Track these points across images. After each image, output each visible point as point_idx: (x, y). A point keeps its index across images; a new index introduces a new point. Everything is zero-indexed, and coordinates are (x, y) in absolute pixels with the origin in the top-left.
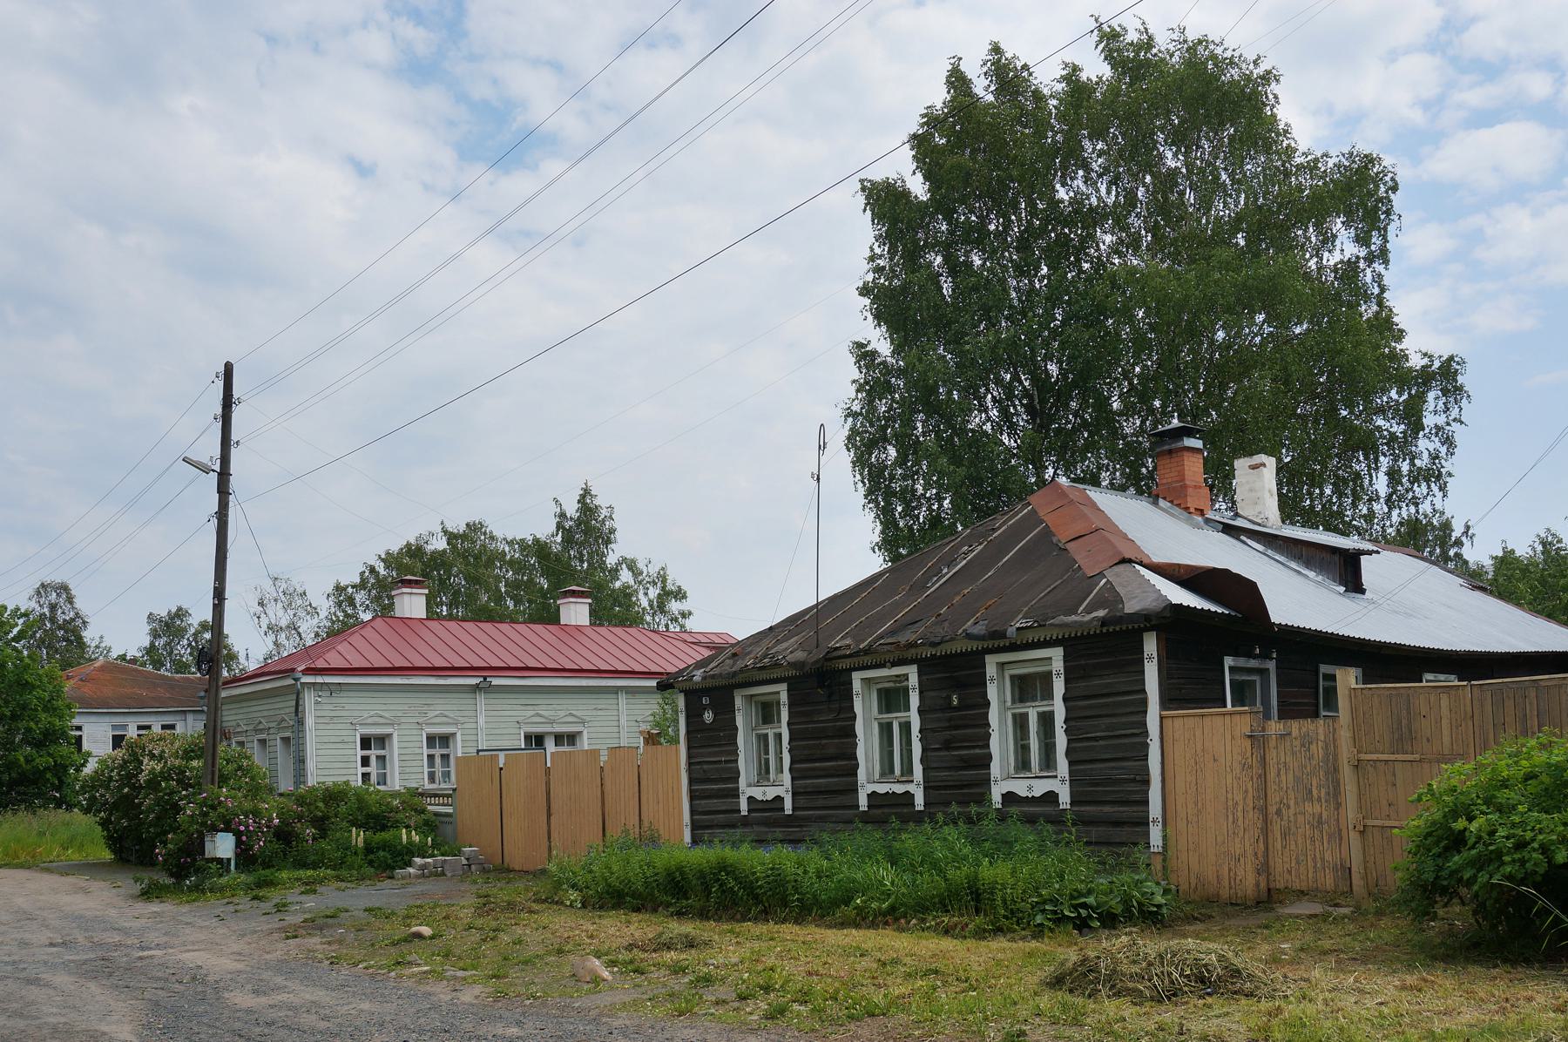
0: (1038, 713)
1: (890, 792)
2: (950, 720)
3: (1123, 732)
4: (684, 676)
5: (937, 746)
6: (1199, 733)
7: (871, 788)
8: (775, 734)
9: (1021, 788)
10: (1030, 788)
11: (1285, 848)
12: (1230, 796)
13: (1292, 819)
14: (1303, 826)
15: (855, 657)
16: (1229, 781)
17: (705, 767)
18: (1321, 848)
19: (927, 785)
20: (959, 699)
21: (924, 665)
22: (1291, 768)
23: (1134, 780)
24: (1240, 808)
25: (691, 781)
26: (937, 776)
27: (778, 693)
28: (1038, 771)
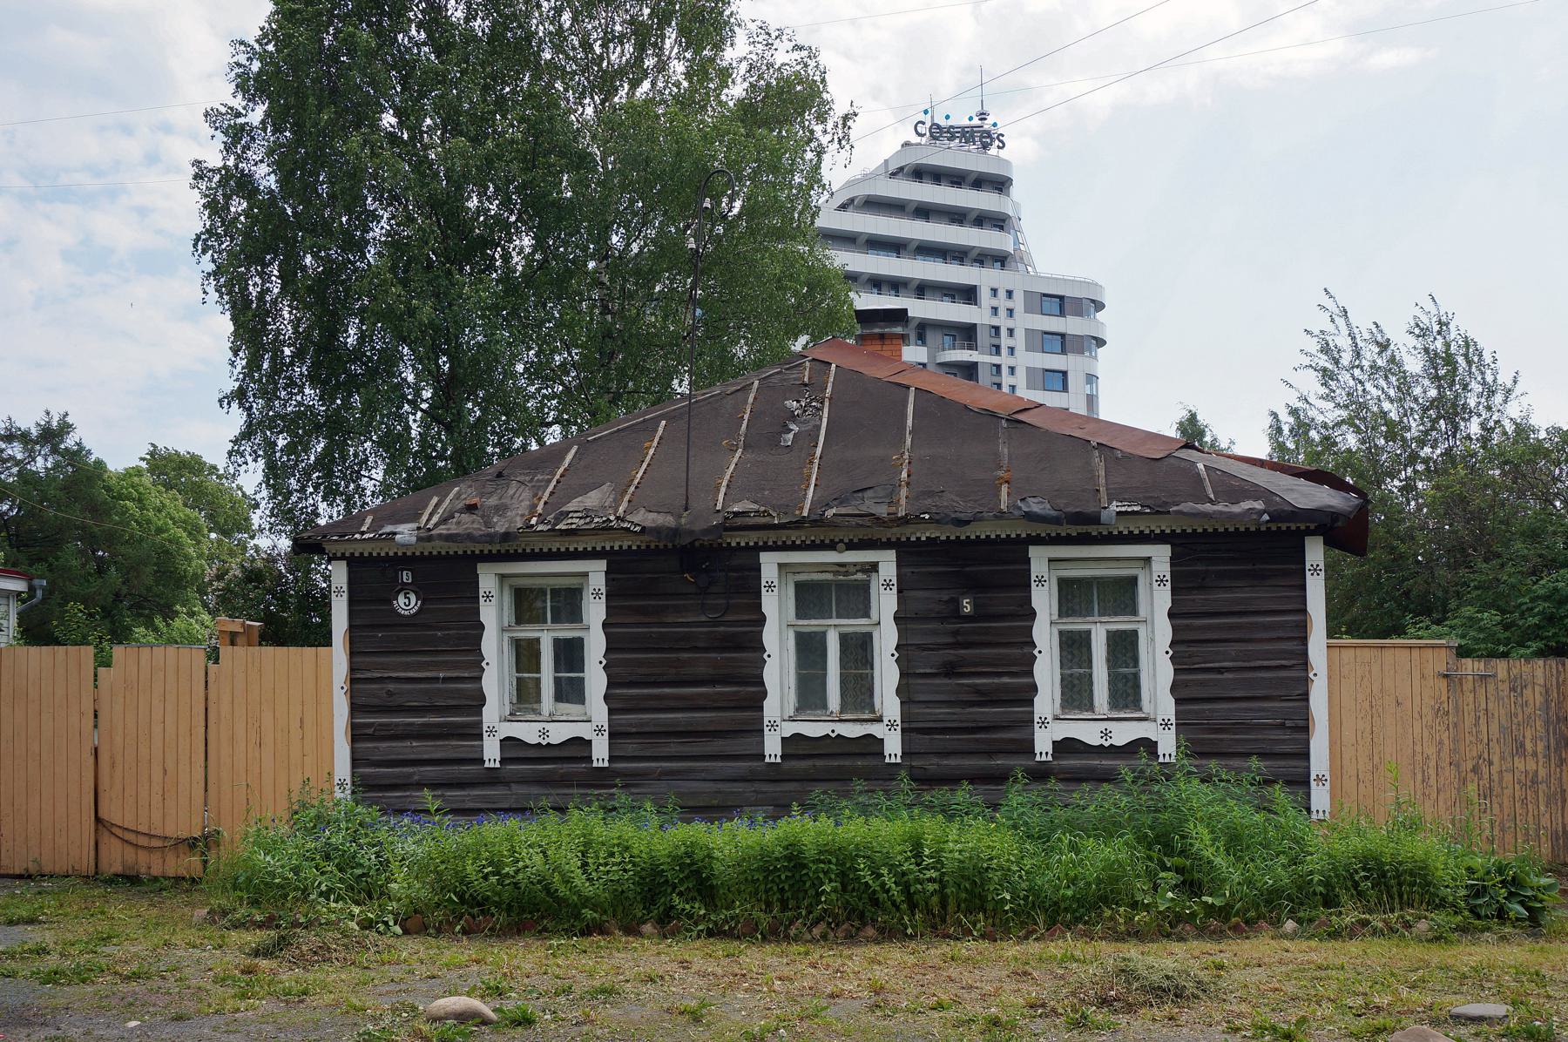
0: (1108, 632)
3: (1266, 663)
4: (363, 533)
5: (928, 671)
6: (1376, 668)
7: (789, 729)
8: (558, 644)
9: (1090, 734)
10: (1106, 734)
11: (1485, 812)
12: (1418, 748)
13: (1495, 777)
14: (1511, 786)
15: (790, 528)
16: (1417, 730)
17: (391, 687)
18: (1536, 813)
19: (906, 725)
20: (975, 606)
21: (908, 553)
22: (1496, 715)
23: (1282, 726)
25: (355, 708)
26: (931, 714)
27: (586, 575)
28: (1106, 711)
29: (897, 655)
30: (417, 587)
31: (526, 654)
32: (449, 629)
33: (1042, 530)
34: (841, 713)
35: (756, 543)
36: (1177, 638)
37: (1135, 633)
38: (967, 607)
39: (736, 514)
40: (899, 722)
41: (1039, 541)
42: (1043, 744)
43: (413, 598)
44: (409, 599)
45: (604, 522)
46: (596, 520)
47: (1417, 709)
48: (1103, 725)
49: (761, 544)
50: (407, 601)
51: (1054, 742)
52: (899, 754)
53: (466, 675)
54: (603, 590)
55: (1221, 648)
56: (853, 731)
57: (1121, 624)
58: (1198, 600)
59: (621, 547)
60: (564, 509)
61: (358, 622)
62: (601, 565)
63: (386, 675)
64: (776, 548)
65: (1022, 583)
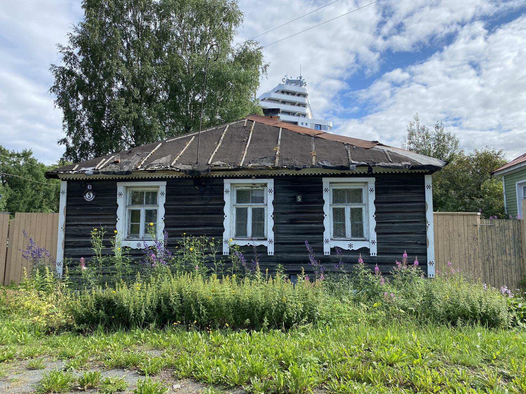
0: (351, 208)
1: (249, 245)
2: (297, 208)
3: (410, 220)
4: (73, 171)
5: (284, 222)
6: (451, 223)
7: (233, 243)
9: (344, 245)
10: (350, 246)
11: (492, 275)
12: (467, 252)
13: (495, 262)
14: (501, 266)
16: (466, 245)
17: (81, 228)
18: (511, 275)
20: (303, 199)
21: (277, 179)
22: (495, 239)
23: (416, 243)
24: (472, 257)
25: (66, 236)
26: (285, 237)
27: (158, 187)
29: (273, 216)
30: (93, 191)
31: (134, 216)
32: (105, 206)
33: (328, 172)
34: (252, 237)
35: (223, 176)
36: (378, 211)
37: (361, 209)
38: (299, 199)
39: (215, 166)
40: (273, 240)
41: (326, 176)
42: (327, 249)
43: (91, 194)
44: (90, 195)
45: (165, 168)
46: (163, 167)
47: (466, 237)
48: (349, 242)
49: (224, 176)
50: (89, 196)
51: (331, 249)
52: (273, 252)
53: (110, 223)
54: (165, 192)
55: (394, 214)
56: (258, 243)
57: (356, 206)
58: (385, 197)
59: (172, 177)
60: (152, 163)
61: (70, 204)
62: (165, 183)
63: (79, 223)
64: (230, 178)
65: (320, 191)
